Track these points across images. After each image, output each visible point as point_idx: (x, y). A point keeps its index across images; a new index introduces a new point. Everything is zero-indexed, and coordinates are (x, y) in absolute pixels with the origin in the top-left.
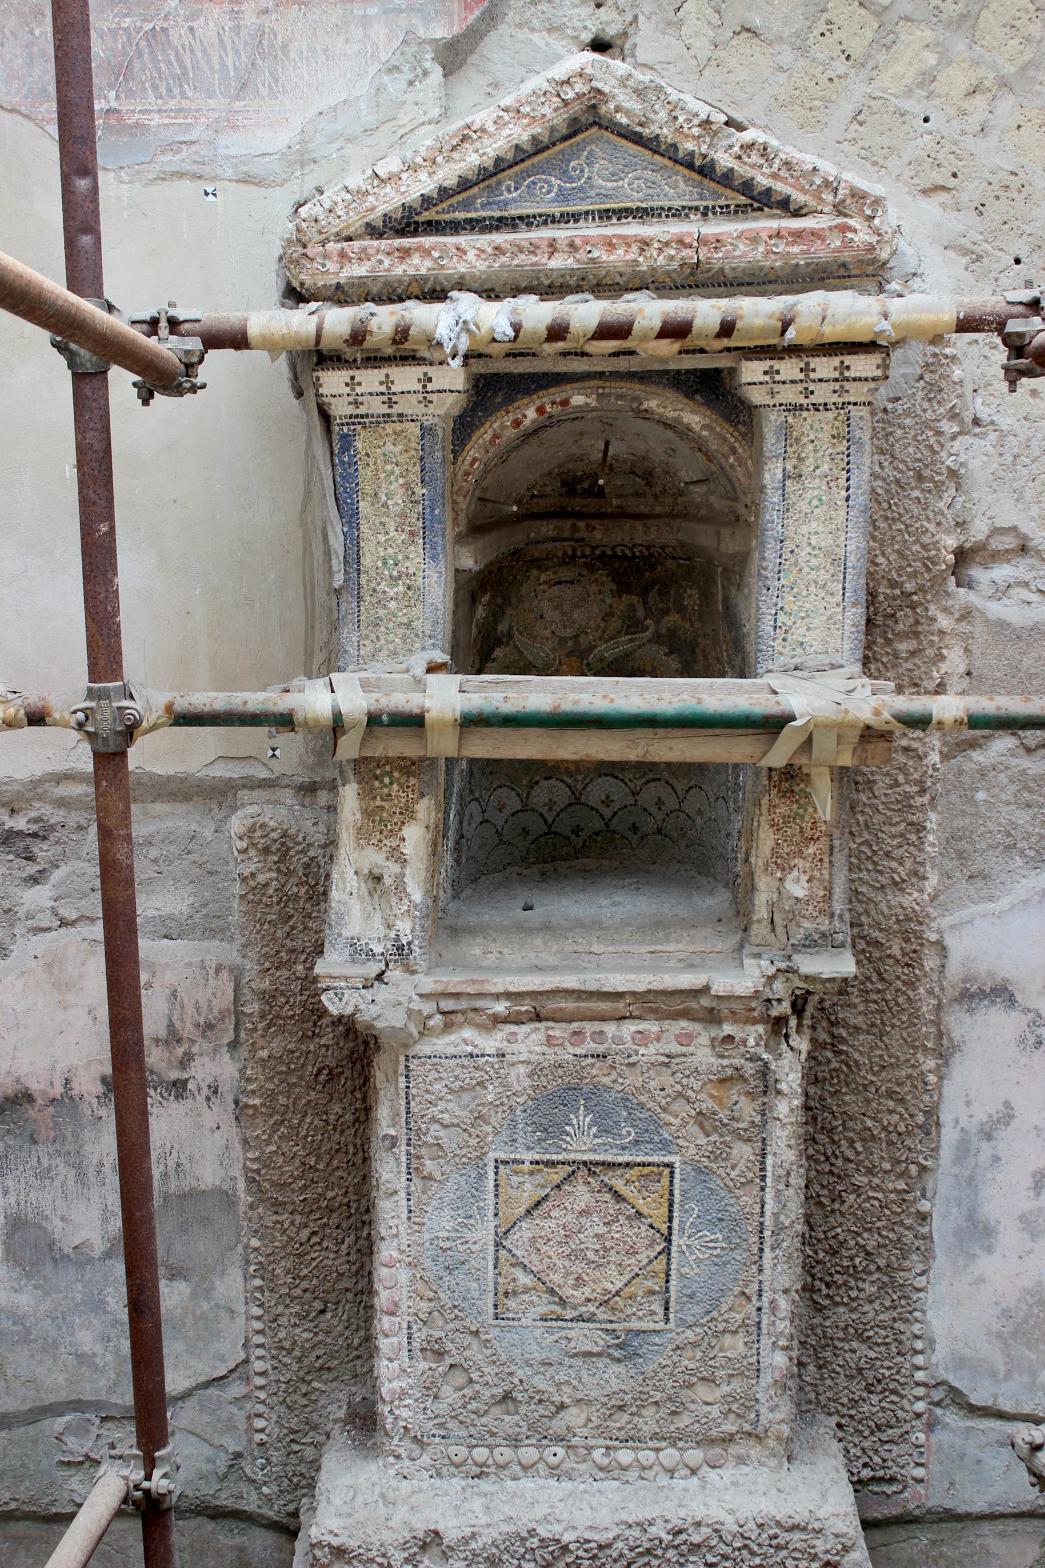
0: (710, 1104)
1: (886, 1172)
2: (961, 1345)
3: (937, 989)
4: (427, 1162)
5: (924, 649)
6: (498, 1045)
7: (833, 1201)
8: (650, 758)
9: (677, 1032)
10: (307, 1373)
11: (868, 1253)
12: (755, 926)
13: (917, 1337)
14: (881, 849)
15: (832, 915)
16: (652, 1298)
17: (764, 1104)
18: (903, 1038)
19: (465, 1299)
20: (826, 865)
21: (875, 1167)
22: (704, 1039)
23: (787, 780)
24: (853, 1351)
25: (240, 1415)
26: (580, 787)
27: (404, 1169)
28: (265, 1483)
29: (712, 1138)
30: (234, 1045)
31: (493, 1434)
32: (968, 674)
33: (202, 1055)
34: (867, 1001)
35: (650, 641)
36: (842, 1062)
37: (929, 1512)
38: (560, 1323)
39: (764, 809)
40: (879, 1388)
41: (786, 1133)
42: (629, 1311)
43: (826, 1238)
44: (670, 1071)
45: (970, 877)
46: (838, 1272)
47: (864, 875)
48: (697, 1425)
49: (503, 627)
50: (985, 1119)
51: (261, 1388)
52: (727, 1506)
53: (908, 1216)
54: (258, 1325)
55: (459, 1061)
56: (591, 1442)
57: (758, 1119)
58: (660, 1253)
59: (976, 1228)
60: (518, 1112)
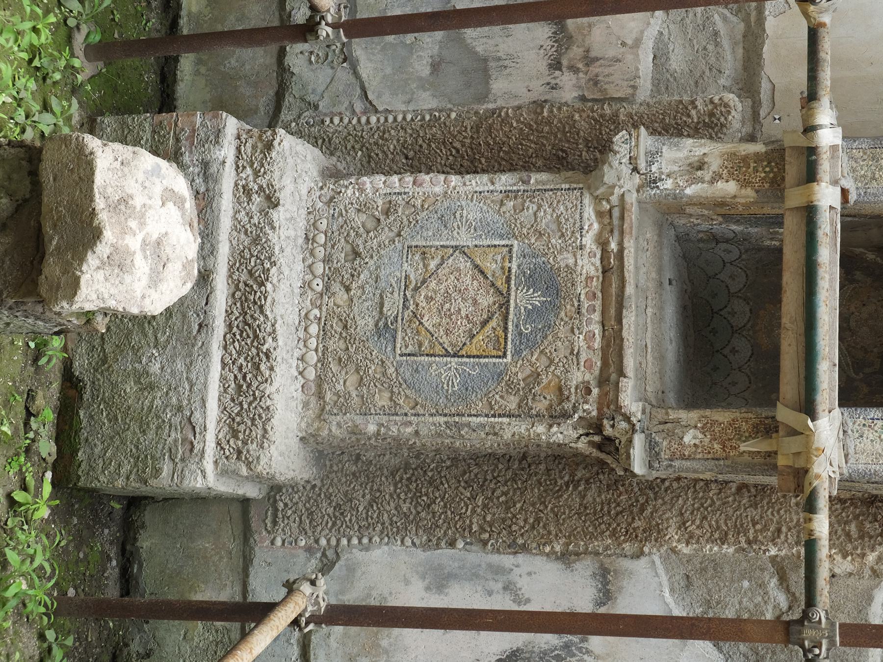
0: (545, 381)
1: (484, 517)
2: (363, 569)
3: (609, 552)
4: (512, 203)
5: (851, 543)
6: (588, 246)
7: (466, 482)
8: (783, 332)
9: (594, 360)
10: (367, 148)
11: (429, 506)
12: (664, 411)
13: (370, 540)
14: (709, 513)
15: (671, 460)
16: (416, 346)
17: (544, 416)
18: (576, 528)
19: (422, 227)
20: (706, 456)
21: (488, 509)
22: (588, 377)
23: (765, 429)
24: (363, 496)
25: (342, 109)
26: (744, 333)
27: (508, 188)
28: (298, 124)
29: (522, 382)
30: (583, 99)
31: (333, 247)
32: (833, 576)
33: (577, 79)
34: (602, 503)
35: (848, 376)
36: (561, 487)
37: (252, 549)
38: (403, 287)
39: (745, 415)
40: (337, 514)
41: (523, 431)
42: (408, 331)
43: (441, 477)
44: (567, 355)
45: (688, 576)
46: (417, 485)
47: (690, 501)
48: (331, 375)
49: (858, 275)
50: (518, 586)
51: (359, 121)
52: (281, 389)
53: (454, 533)
54: (400, 118)
55: (578, 221)
56: (324, 309)
57: (534, 412)
58: (446, 350)
59: (443, 579)
60: (543, 259)
